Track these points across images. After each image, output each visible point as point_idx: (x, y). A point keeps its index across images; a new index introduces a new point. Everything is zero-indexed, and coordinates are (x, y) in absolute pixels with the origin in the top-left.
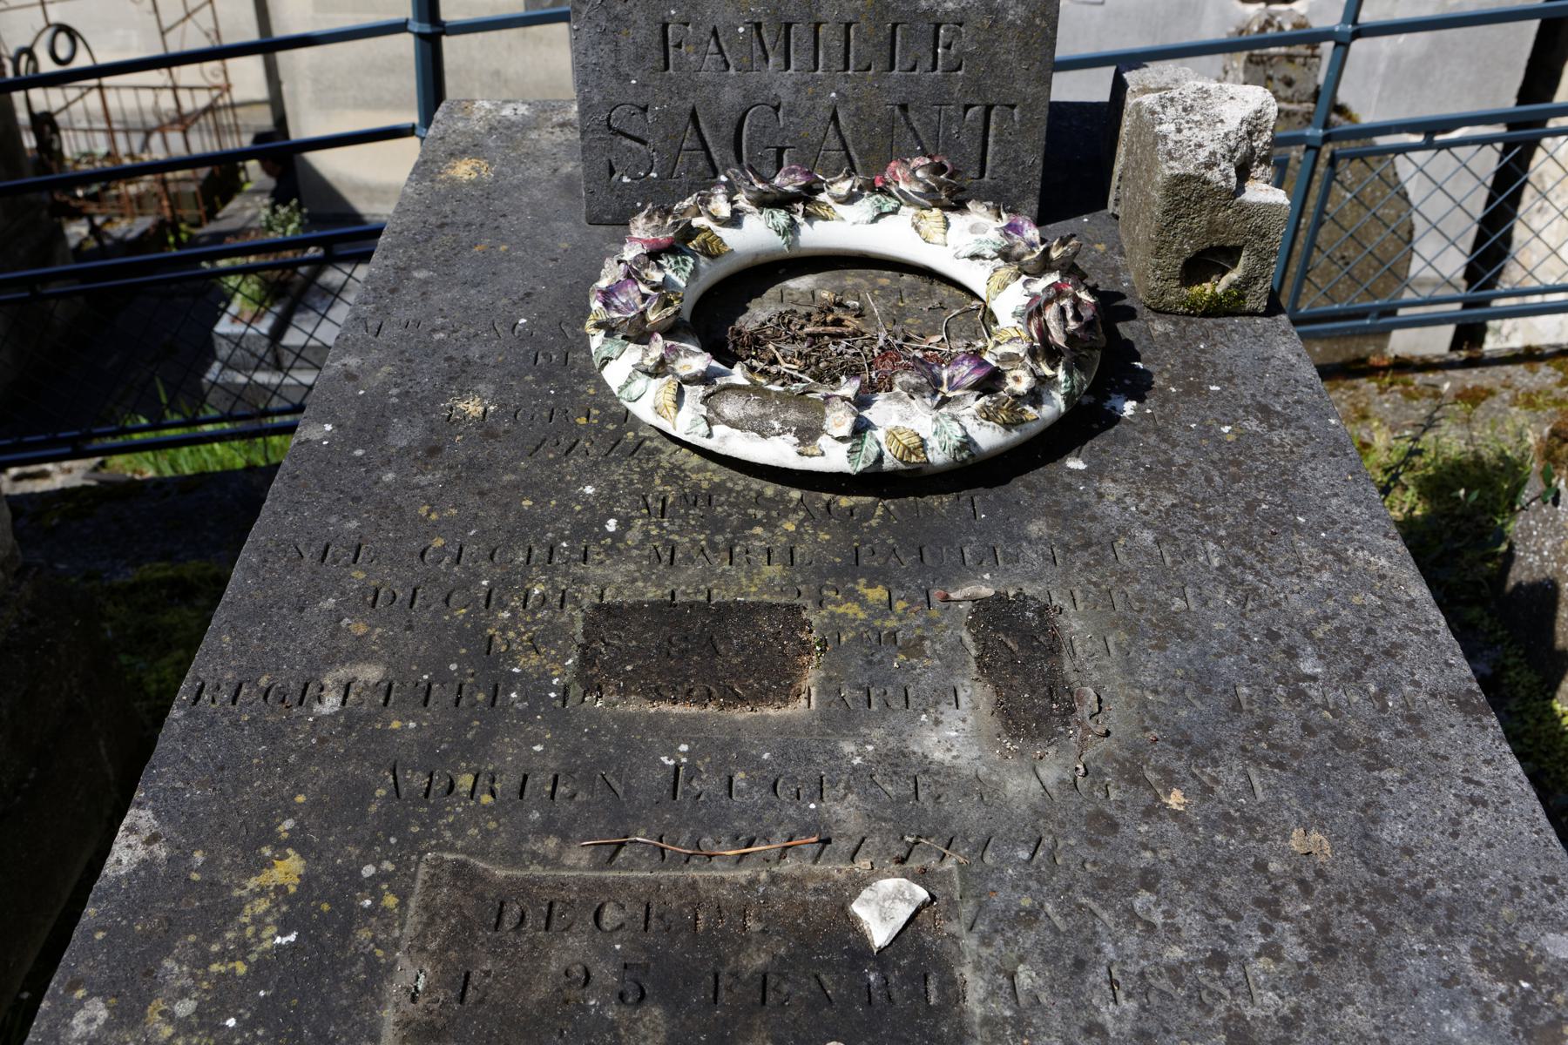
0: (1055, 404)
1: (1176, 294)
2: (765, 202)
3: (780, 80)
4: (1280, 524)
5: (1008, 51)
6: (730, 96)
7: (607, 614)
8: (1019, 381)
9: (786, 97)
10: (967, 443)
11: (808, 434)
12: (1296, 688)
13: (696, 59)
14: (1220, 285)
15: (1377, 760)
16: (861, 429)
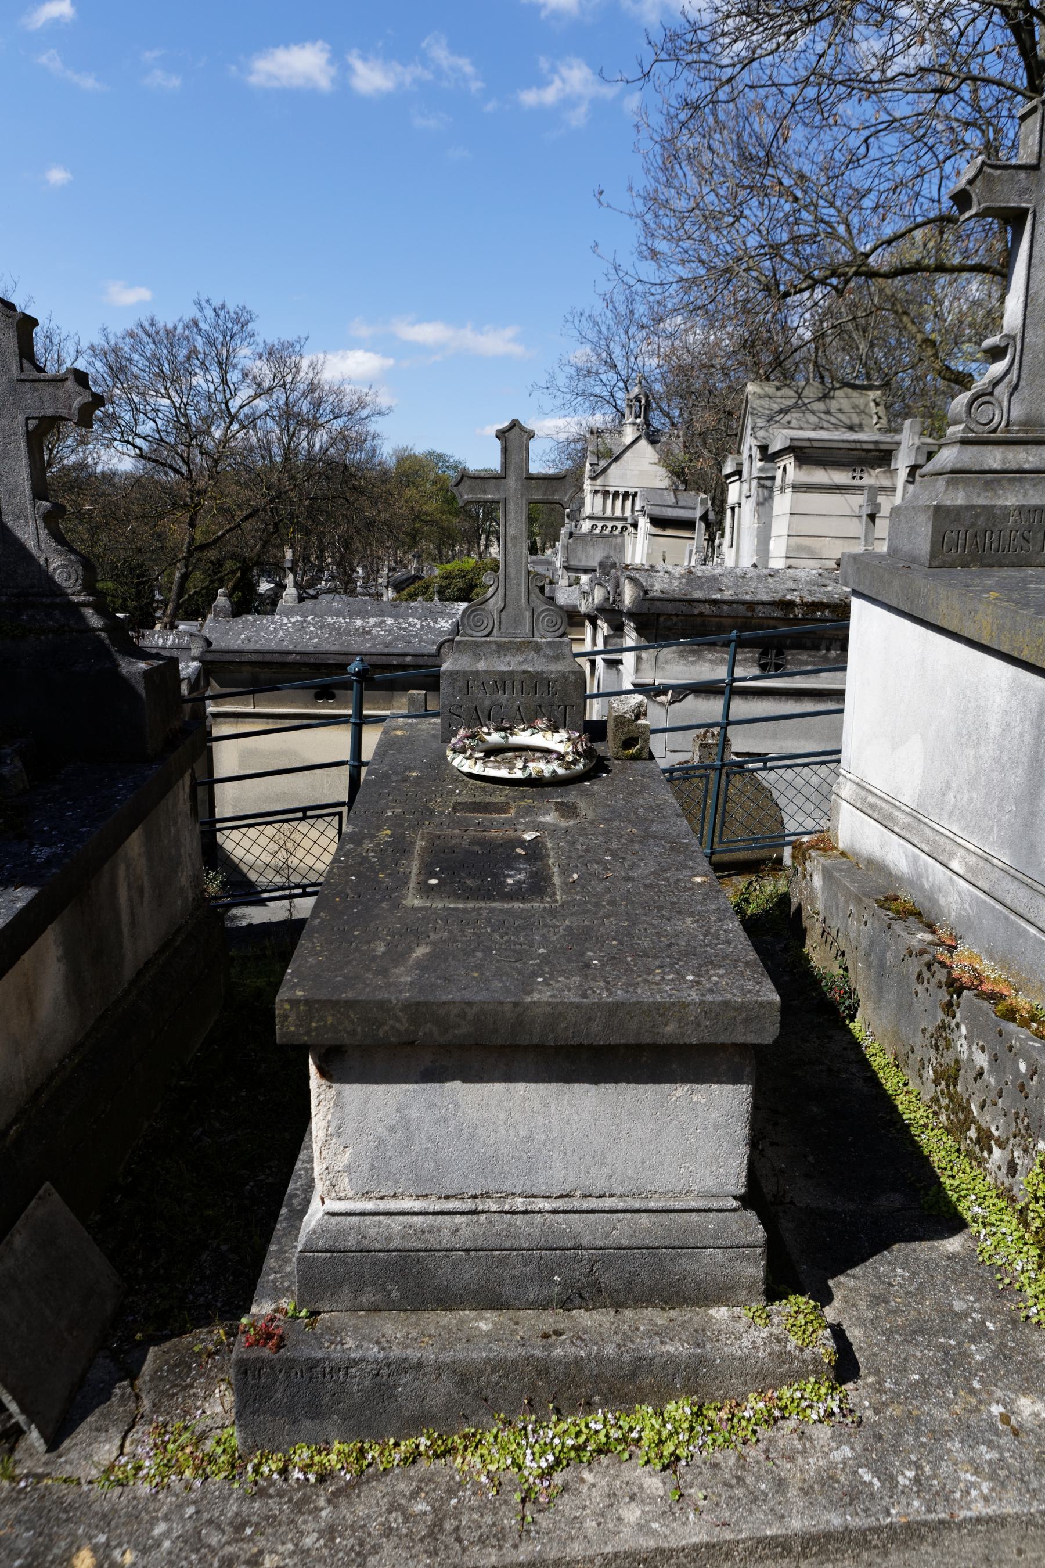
0: (580, 767)
1: (622, 753)
2: (497, 730)
3: (503, 698)
4: (639, 792)
5: (570, 689)
6: (487, 702)
7: (456, 804)
8: (570, 758)
9: (504, 703)
10: (554, 771)
11: (511, 769)
12: (636, 813)
13: (477, 691)
14: (633, 750)
15: (652, 821)
16: (525, 767)
